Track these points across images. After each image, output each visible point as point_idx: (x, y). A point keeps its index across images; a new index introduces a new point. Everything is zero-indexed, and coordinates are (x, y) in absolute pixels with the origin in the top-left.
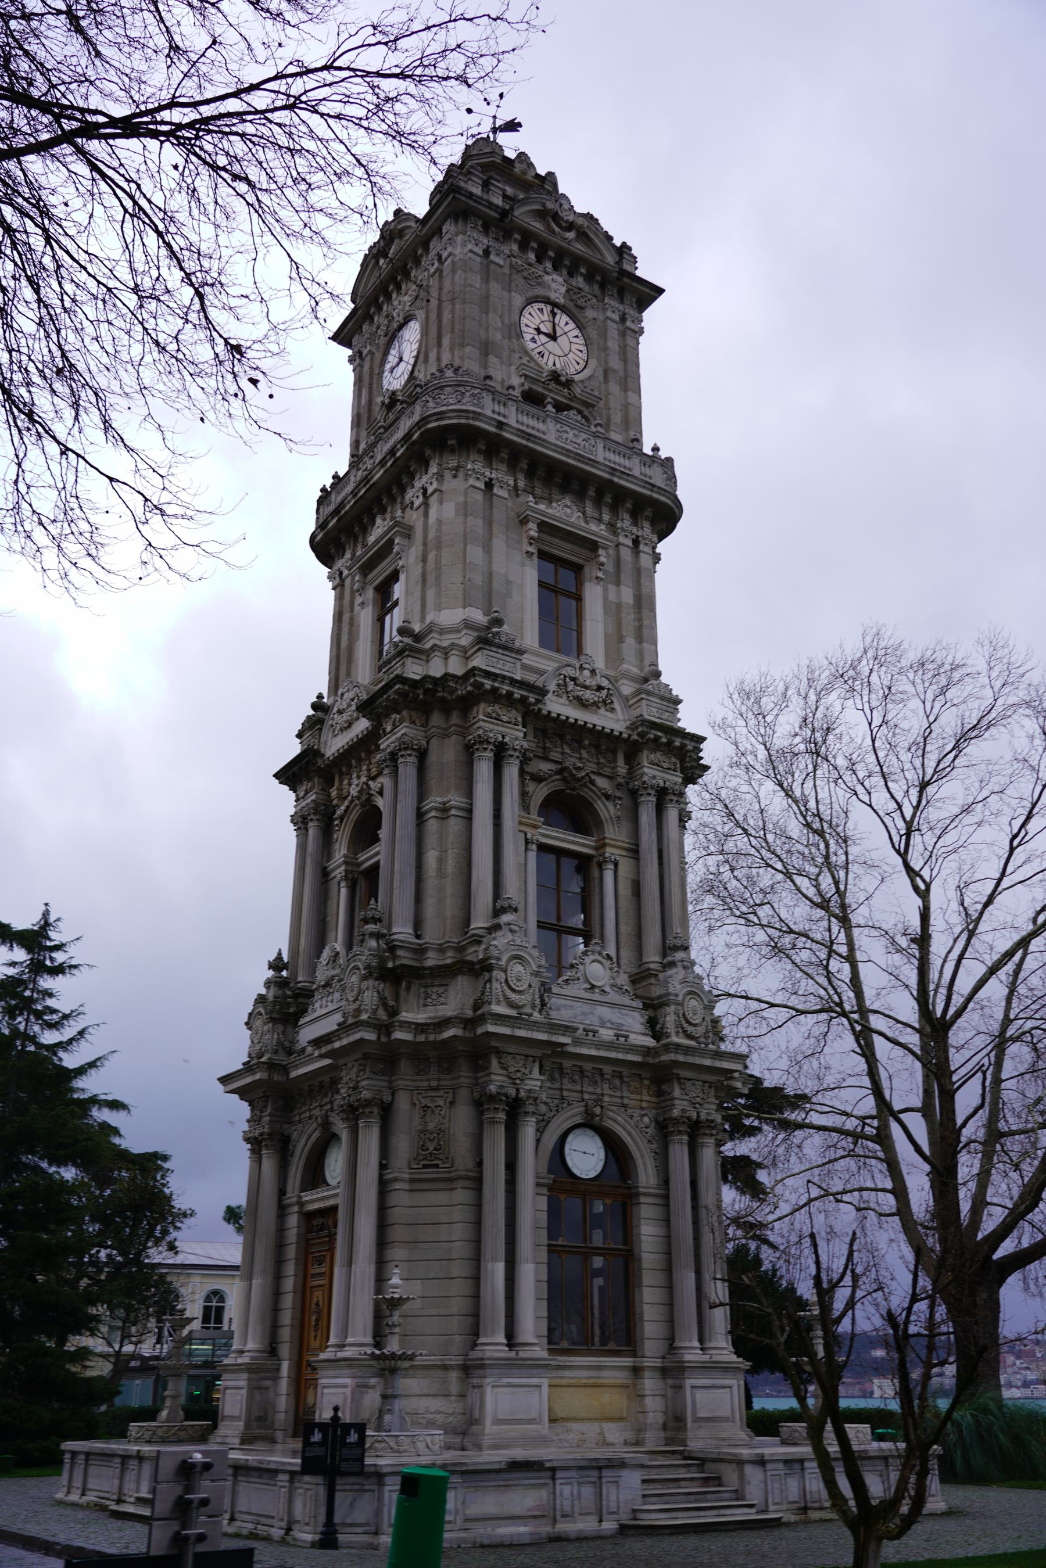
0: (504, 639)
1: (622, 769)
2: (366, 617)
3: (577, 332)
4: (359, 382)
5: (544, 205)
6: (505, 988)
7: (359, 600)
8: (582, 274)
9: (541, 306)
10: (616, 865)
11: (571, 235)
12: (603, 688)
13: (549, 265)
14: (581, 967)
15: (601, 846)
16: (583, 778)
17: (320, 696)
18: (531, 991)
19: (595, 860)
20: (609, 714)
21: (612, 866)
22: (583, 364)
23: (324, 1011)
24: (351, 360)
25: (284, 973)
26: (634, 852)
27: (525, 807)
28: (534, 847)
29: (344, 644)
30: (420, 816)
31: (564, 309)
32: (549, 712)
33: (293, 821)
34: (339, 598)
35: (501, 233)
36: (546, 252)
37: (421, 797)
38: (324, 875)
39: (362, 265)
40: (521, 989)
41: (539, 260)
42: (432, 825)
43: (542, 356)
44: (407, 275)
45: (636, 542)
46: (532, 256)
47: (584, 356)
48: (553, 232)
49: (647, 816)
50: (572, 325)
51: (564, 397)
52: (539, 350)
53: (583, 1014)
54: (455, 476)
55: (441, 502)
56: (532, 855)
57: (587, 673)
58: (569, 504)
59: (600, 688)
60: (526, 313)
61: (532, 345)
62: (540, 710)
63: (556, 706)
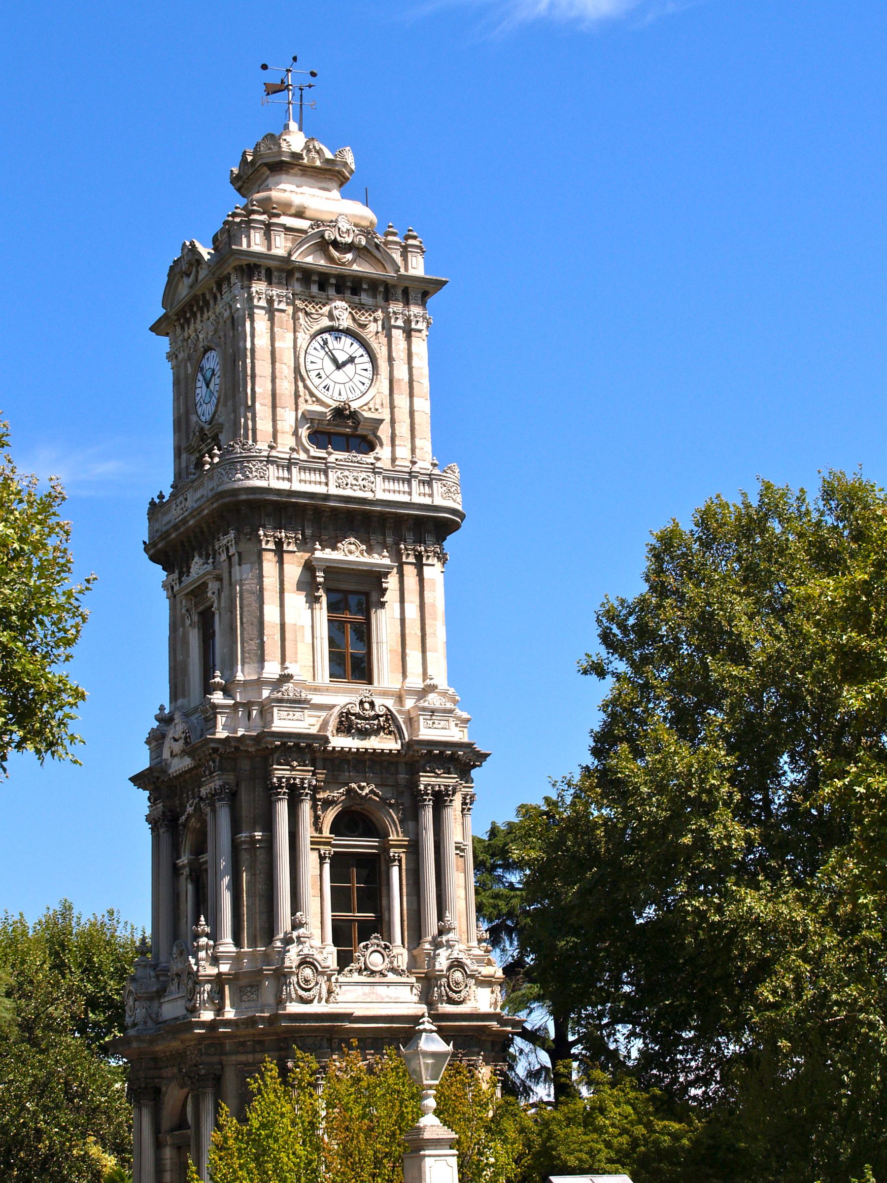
0: (291, 694)
1: (402, 777)
2: (194, 638)
3: (361, 351)
4: (177, 382)
5: (323, 237)
6: (297, 988)
7: (188, 622)
8: (365, 290)
9: (326, 336)
10: (400, 861)
11: (349, 256)
12: (382, 716)
13: (332, 292)
14: (362, 959)
15: (385, 847)
16: (367, 794)
17: (162, 708)
18: (318, 987)
19: (382, 858)
20: (389, 737)
21: (397, 863)
22: (367, 382)
23: (177, 996)
24: (171, 356)
25: (149, 956)
26: (414, 849)
27: (318, 828)
28: (328, 861)
29: (180, 658)
30: (235, 847)
31: (348, 332)
32: (334, 748)
33: (148, 819)
34: (173, 608)
35: (284, 275)
36: (328, 280)
37: (236, 828)
38: (176, 870)
39: (169, 275)
40: (309, 987)
41: (322, 287)
42: (245, 857)
43: (328, 390)
44: (207, 303)
45: (419, 557)
46: (314, 289)
47: (369, 374)
48: (331, 259)
49: (428, 815)
50: (356, 346)
51: (349, 427)
52: (324, 385)
53: (364, 994)
54: (250, 539)
55: (240, 565)
56: (327, 867)
57: (367, 706)
58: (352, 540)
59: (377, 716)
60: (311, 350)
61: (317, 381)
62: (325, 748)
63: (340, 742)
